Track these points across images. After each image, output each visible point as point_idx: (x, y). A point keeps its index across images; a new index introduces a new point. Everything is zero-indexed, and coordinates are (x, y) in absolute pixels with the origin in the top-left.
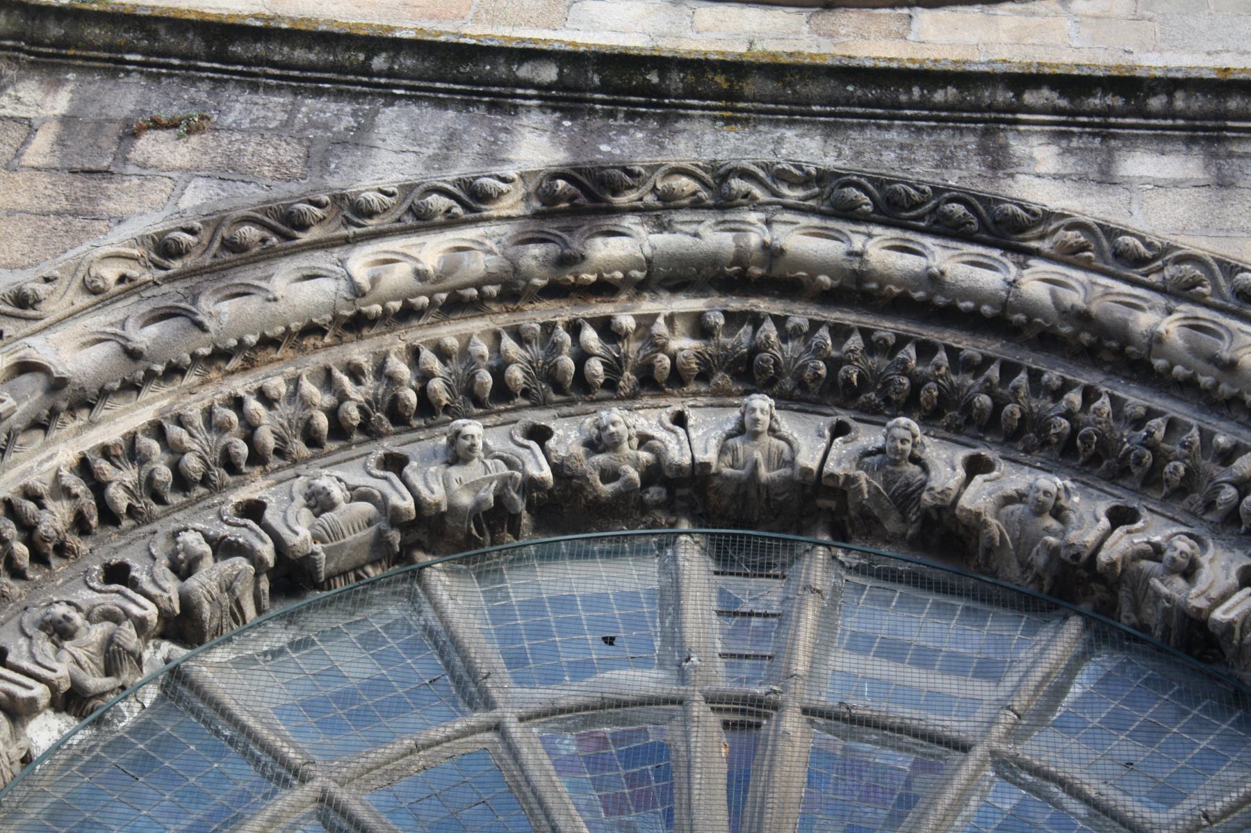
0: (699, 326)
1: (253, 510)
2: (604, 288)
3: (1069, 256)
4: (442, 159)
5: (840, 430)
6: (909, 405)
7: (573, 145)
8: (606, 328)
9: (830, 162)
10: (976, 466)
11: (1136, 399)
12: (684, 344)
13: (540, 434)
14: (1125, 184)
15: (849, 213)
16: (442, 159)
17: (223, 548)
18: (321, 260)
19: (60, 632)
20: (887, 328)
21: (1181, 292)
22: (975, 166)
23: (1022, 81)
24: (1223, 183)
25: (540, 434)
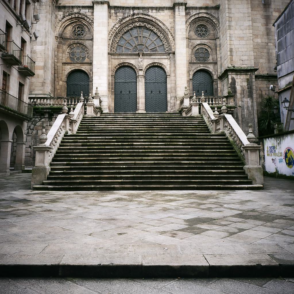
0: (138, 20)
1: (124, 30)
2: (134, 19)
3: (151, 17)
4: (128, 14)
5: (143, 23)
6: (145, 22)
7: (133, 12)
8: (134, 20)
9: (142, 12)
10: (148, 25)
11: (153, 23)
12: (137, 20)
13: (133, 25)
14: (153, 12)
15: (143, 15)
16: (128, 14)
17: (123, 32)
18: (125, 20)
19: (119, 37)
20: (144, 20)
21: (155, 19)
22: (147, 11)
23: (149, 7)
24: (157, 12)
25: (133, 25)
